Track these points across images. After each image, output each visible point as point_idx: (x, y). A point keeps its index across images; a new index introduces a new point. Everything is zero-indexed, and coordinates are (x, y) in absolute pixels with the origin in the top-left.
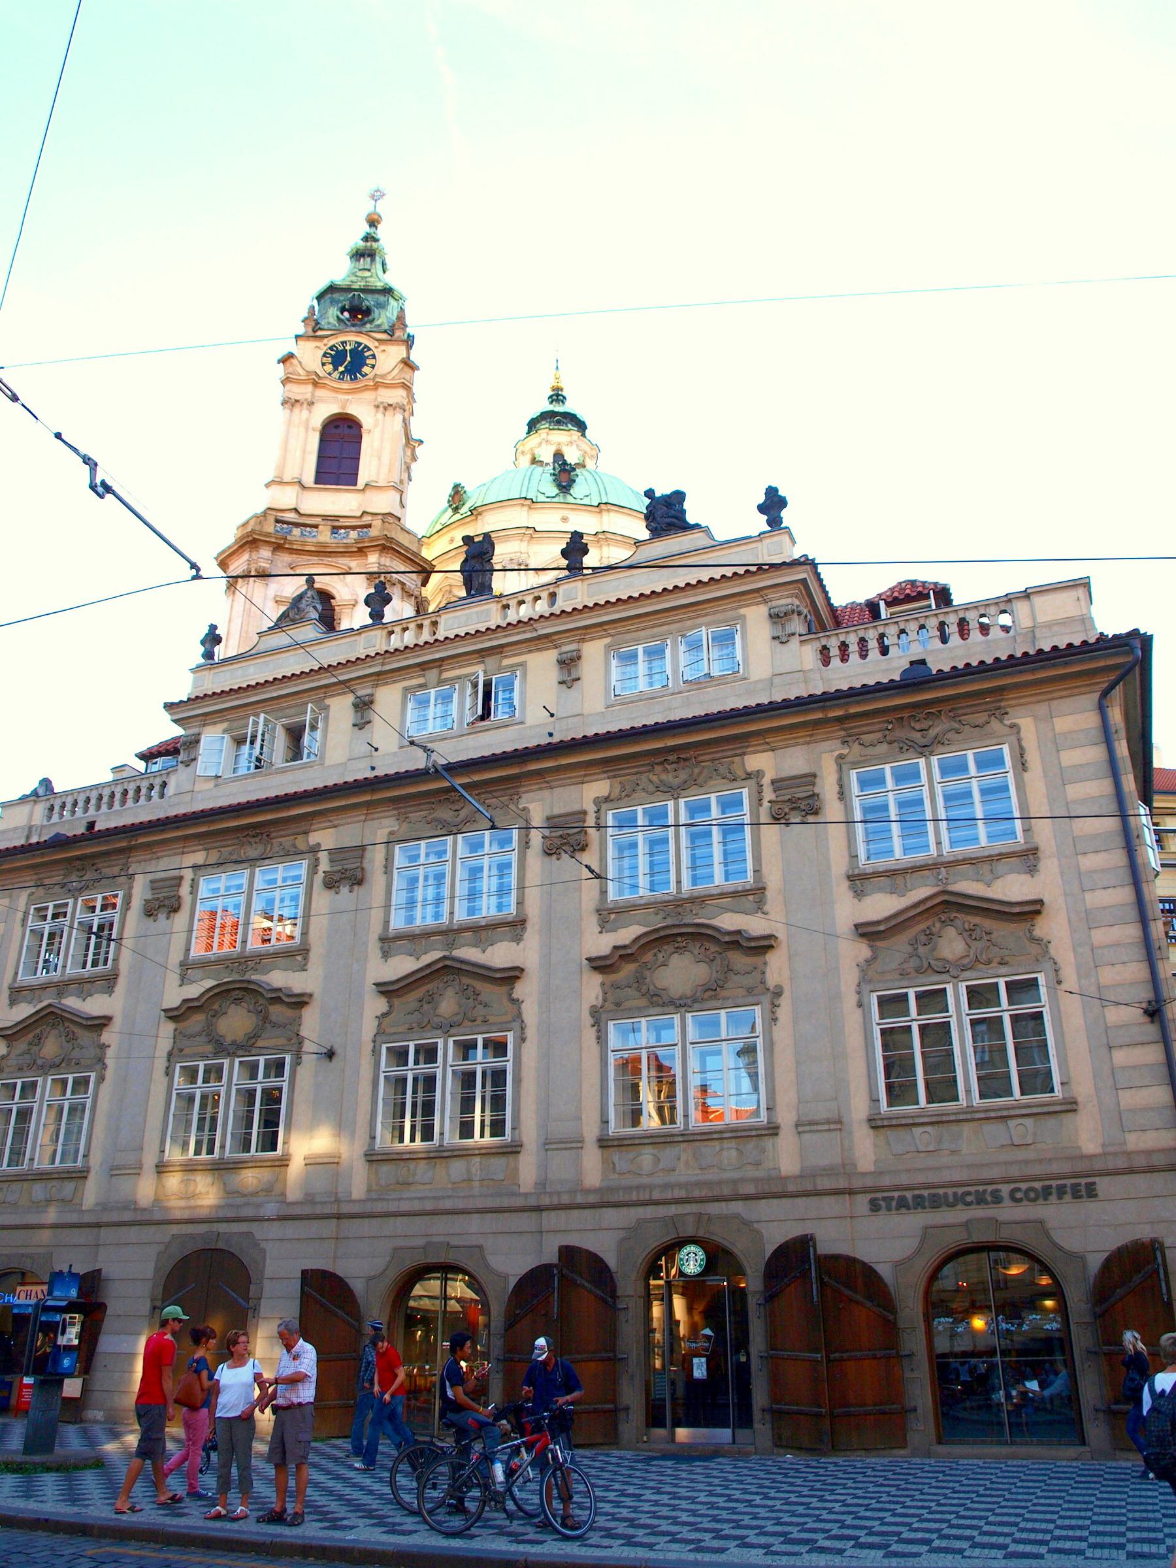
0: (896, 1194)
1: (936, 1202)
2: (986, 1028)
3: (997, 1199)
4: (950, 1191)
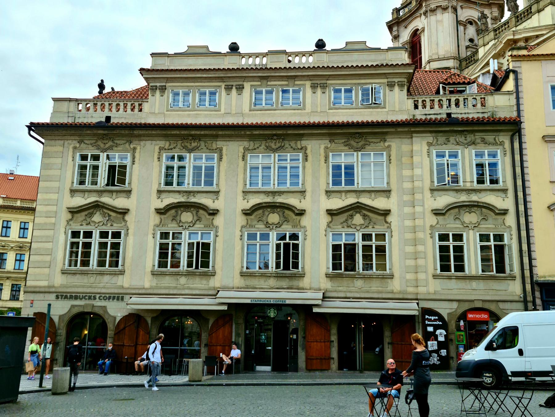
0: (65, 294)
1: (76, 298)
2: (103, 245)
3: (95, 298)
4: (81, 295)
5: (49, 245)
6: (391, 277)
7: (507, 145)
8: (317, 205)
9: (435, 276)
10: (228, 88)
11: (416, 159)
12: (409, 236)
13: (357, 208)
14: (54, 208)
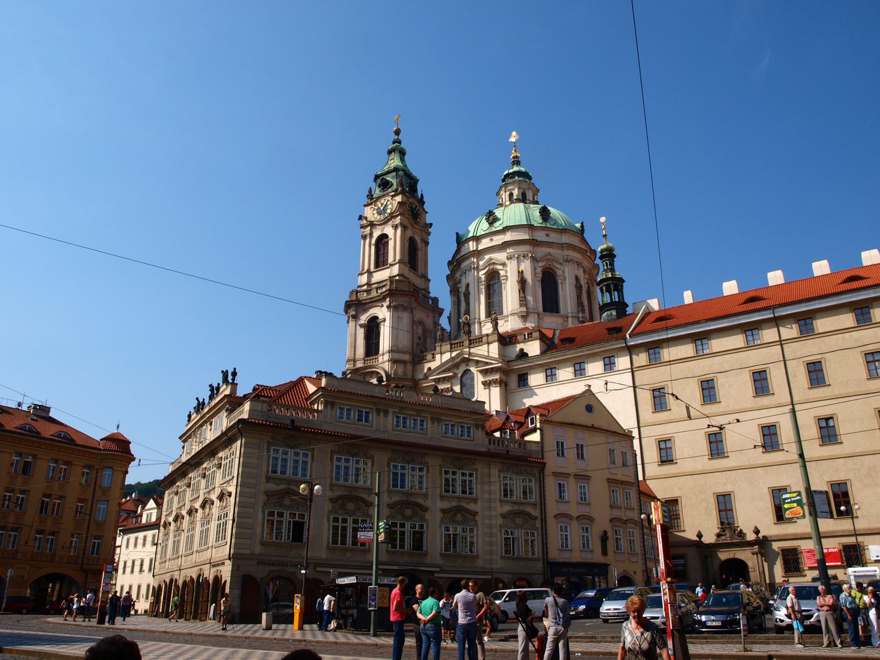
1: (273, 564)
3: (287, 565)
5: (250, 521)
6: (477, 557)
7: (537, 475)
8: (436, 505)
9: (502, 557)
10: (378, 411)
11: (492, 479)
12: (487, 530)
13: (459, 509)
14: (253, 490)
